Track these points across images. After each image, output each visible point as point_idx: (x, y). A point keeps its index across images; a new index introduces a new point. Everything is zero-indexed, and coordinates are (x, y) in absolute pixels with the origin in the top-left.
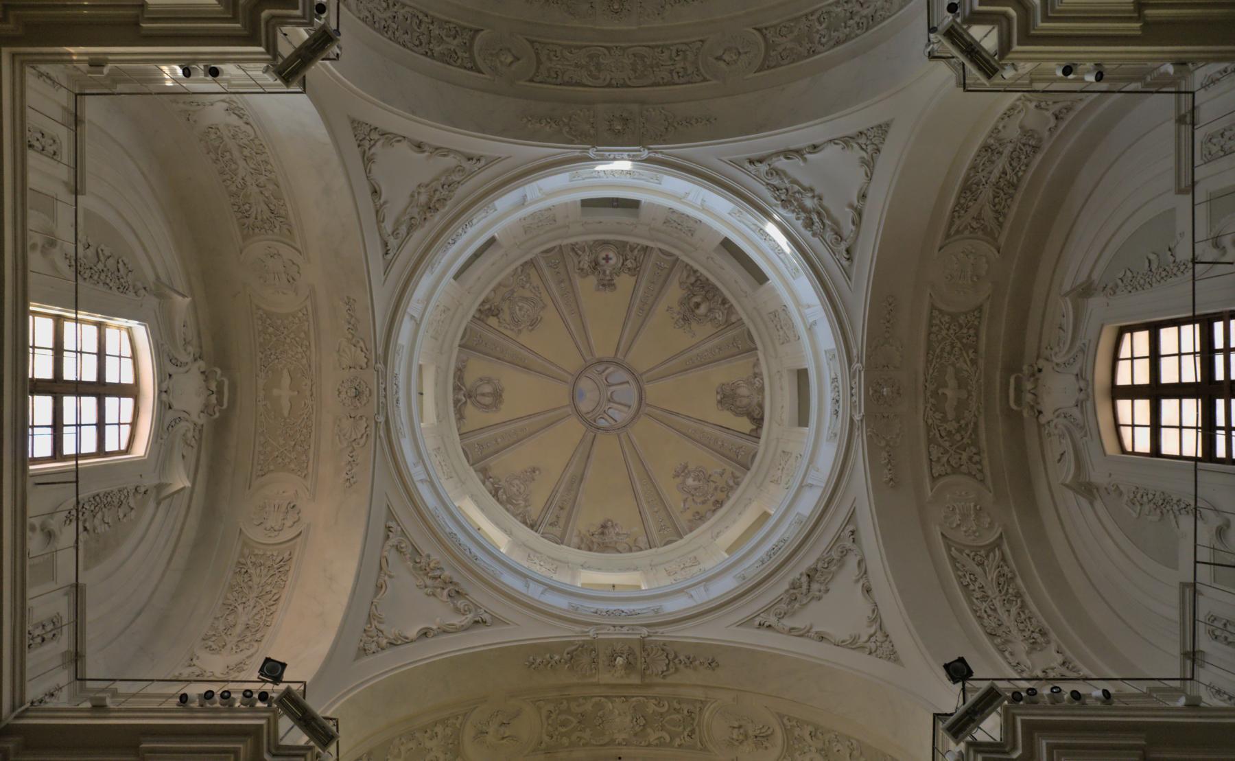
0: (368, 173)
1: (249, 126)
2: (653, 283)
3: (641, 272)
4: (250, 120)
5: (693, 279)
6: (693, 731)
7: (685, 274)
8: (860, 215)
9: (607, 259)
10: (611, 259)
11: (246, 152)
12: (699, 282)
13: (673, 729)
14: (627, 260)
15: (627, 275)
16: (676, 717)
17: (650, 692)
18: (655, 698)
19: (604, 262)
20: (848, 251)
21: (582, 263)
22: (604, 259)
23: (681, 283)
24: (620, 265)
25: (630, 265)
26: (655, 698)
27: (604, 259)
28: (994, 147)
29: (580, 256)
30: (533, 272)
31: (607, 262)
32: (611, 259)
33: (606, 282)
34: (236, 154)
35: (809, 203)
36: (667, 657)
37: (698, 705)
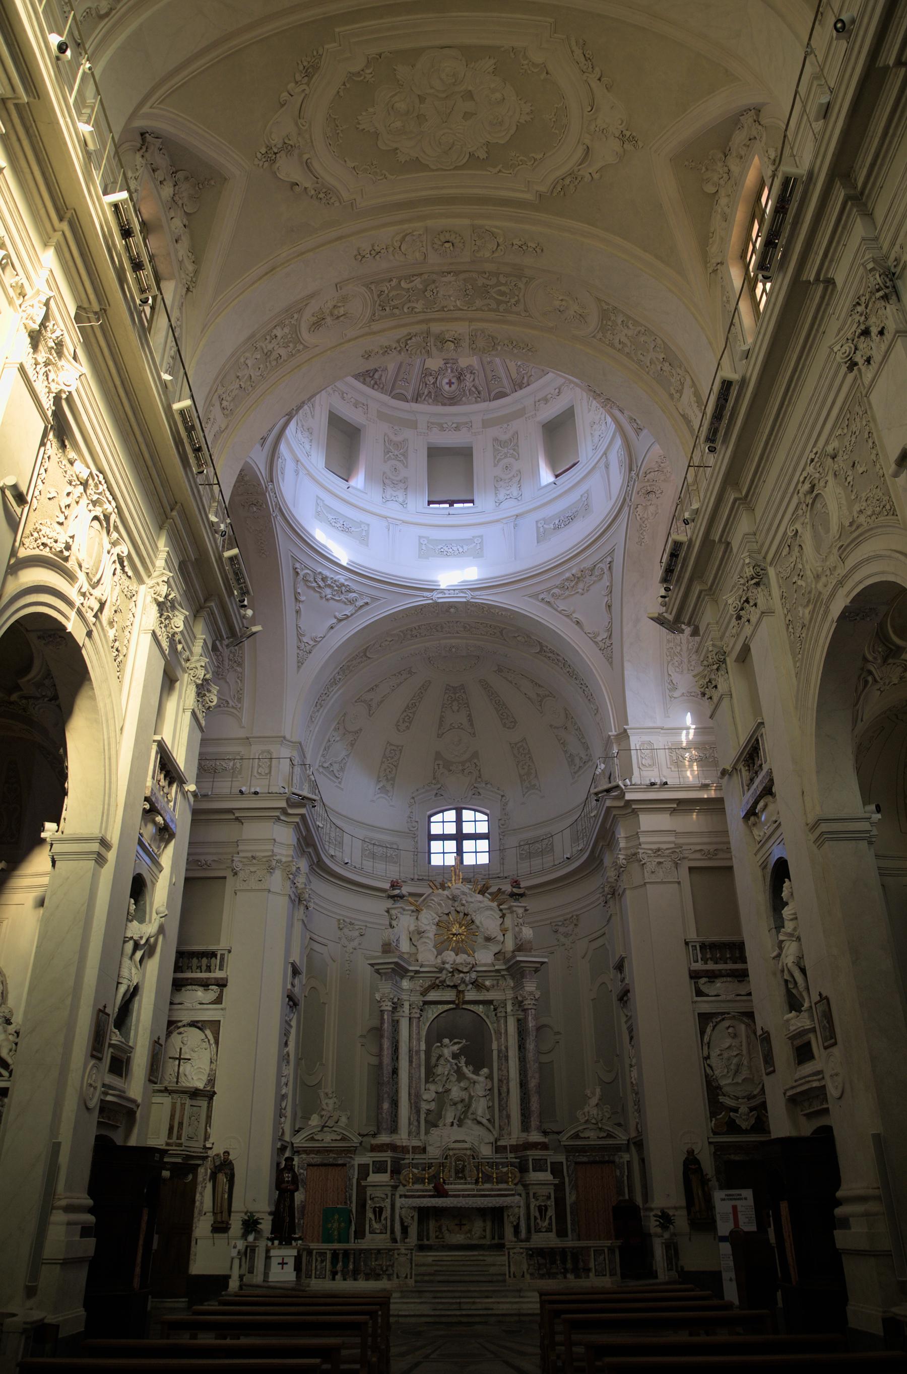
0: (611, 623)
1: (670, 673)
2: (410, 365)
3: (421, 372)
4: (666, 678)
5: (376, 376)
6: (379, 296)
7: (383, 379)
8: (296, 598)
9: (450, 383)
10: (447, 383)
11: (679, 648)
12: (371, 375)
13: (398, 292)
14: (433, 383)
15: (432, 369)
16: (396, 302)
17: (421, 317)
18: (416, 313)
19: (454, 380)
20: (297, 573)
21: (472, 379)
22: (453, 383)
23: (386, 369)
24: (439, 377)
25: (431, 378)
26: (416, 313)
27: (453, 383)
28: (235, 664)
29: (473, 386)
30: (514, 375)
31: (450, 380)
32: (447, 383)
33: (451, 361)
34: (685, 648)
35: (328, 591)
36: (407, 350)
37: (377, 318)
